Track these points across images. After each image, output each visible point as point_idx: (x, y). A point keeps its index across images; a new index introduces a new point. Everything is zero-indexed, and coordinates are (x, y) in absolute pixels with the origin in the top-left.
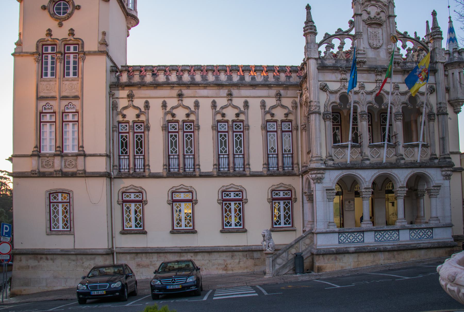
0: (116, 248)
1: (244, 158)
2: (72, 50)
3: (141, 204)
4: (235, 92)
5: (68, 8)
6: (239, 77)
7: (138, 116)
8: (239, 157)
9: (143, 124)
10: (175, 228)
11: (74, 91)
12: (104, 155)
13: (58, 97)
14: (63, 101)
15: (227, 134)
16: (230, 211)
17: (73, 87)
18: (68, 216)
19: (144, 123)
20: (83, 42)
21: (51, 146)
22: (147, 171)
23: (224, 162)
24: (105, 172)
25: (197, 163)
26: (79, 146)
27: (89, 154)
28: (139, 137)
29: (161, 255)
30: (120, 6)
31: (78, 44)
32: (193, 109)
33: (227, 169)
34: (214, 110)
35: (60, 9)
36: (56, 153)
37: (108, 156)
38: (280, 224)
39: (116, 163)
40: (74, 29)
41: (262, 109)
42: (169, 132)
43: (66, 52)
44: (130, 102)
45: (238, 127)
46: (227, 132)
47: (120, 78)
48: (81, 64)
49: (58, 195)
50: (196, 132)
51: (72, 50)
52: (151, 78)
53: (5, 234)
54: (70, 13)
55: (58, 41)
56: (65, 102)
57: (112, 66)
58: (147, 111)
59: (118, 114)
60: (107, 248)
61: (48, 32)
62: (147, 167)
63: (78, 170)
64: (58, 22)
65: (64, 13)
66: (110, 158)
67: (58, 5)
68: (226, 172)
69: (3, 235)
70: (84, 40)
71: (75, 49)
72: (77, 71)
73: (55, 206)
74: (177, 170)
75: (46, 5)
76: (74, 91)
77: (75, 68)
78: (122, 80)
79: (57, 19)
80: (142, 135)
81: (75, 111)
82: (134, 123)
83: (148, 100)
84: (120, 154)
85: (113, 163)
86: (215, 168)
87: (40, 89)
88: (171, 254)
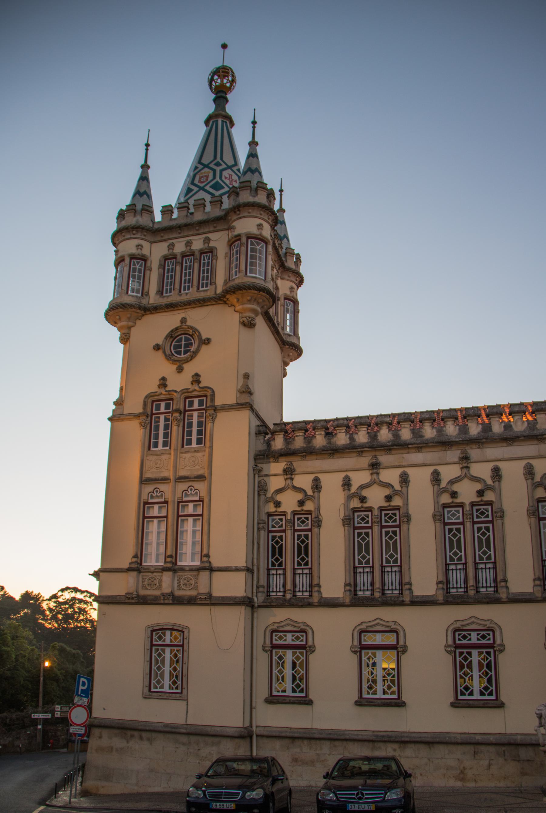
0: (257, 727)
1: (495, 568)
2: (196, 405)
3: (304, 651)
4: (474, 453)
5: (191, 344)
6: (480, 426)
8: (486, 568)
9: (309, 516)
10: (365, 696)
11: (197, 467)
12: (243, 568)
13: (172, 478)
14: (179, 484)
15: (461, 527)
16: (470, 666)
17: (196, 462)
18: (179, 669)
19: (311, 514)
20: (213, 392)
21: (158, 555)
22: (315, 594)
23: (456, 577)
24: (245, 597)
25: (406, 579)
26: (203, 554)
27: (218, 567)
28: (303, 537)
29: (338, 743)
30: (272, 332)
31: (206, 396)
32: (397, 487)
33: (462, 590)
34: (436, 487)
36: (165, 566)
37: (249, 570)
39: (263, 582)
40: (200, 373)
41: (526, 480)
42: (355, 528)
43: (187, 408)
44: (289, 481)
45: (482, 513)
46: (462, 523)
47: (272, 443)
49: (165, 632)
50: (404, 527)
51: (196, 405)
52: (324, 439)
53: (81, 693)
54: (194, 350)
55: (175, 394)
57: (258, 426)
58: (316, 494)
59: (267, 501)
60: (242, 726)
61: (162, 381)
62: (316, 589)
63: (199, 594)
64: (177, 366)
65: (186, 352)
66: (253, 574)
67: (178, 341)
68: (461, 595)
69: (77, 694)
70: (214, 389)
71: (201, 403)
72: (203, 436)
73: (160, 651)
74: (368, 593)
75: (160, 343)
76: (197, 467)
77: (199, 433)
78: (275, 446)
79: (174, 362)
80: (308, 535)
81: (197, 498)
82: (294, 515)
83: (319, 475)
84: (270, 567)
85: (258, 582)
86: (439, 589)
87: (146, 468)
88: (356, 744)
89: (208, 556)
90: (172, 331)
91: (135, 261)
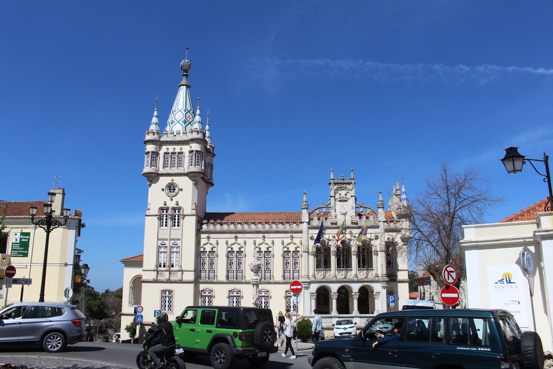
7: (212, 249)
35: (171, 189)
40: (178, 201)
56: (173, 241)
65: (173, 192)
75: (164, 188)
85: (197, 274)
89: (181, 266)
90: (168, 184)
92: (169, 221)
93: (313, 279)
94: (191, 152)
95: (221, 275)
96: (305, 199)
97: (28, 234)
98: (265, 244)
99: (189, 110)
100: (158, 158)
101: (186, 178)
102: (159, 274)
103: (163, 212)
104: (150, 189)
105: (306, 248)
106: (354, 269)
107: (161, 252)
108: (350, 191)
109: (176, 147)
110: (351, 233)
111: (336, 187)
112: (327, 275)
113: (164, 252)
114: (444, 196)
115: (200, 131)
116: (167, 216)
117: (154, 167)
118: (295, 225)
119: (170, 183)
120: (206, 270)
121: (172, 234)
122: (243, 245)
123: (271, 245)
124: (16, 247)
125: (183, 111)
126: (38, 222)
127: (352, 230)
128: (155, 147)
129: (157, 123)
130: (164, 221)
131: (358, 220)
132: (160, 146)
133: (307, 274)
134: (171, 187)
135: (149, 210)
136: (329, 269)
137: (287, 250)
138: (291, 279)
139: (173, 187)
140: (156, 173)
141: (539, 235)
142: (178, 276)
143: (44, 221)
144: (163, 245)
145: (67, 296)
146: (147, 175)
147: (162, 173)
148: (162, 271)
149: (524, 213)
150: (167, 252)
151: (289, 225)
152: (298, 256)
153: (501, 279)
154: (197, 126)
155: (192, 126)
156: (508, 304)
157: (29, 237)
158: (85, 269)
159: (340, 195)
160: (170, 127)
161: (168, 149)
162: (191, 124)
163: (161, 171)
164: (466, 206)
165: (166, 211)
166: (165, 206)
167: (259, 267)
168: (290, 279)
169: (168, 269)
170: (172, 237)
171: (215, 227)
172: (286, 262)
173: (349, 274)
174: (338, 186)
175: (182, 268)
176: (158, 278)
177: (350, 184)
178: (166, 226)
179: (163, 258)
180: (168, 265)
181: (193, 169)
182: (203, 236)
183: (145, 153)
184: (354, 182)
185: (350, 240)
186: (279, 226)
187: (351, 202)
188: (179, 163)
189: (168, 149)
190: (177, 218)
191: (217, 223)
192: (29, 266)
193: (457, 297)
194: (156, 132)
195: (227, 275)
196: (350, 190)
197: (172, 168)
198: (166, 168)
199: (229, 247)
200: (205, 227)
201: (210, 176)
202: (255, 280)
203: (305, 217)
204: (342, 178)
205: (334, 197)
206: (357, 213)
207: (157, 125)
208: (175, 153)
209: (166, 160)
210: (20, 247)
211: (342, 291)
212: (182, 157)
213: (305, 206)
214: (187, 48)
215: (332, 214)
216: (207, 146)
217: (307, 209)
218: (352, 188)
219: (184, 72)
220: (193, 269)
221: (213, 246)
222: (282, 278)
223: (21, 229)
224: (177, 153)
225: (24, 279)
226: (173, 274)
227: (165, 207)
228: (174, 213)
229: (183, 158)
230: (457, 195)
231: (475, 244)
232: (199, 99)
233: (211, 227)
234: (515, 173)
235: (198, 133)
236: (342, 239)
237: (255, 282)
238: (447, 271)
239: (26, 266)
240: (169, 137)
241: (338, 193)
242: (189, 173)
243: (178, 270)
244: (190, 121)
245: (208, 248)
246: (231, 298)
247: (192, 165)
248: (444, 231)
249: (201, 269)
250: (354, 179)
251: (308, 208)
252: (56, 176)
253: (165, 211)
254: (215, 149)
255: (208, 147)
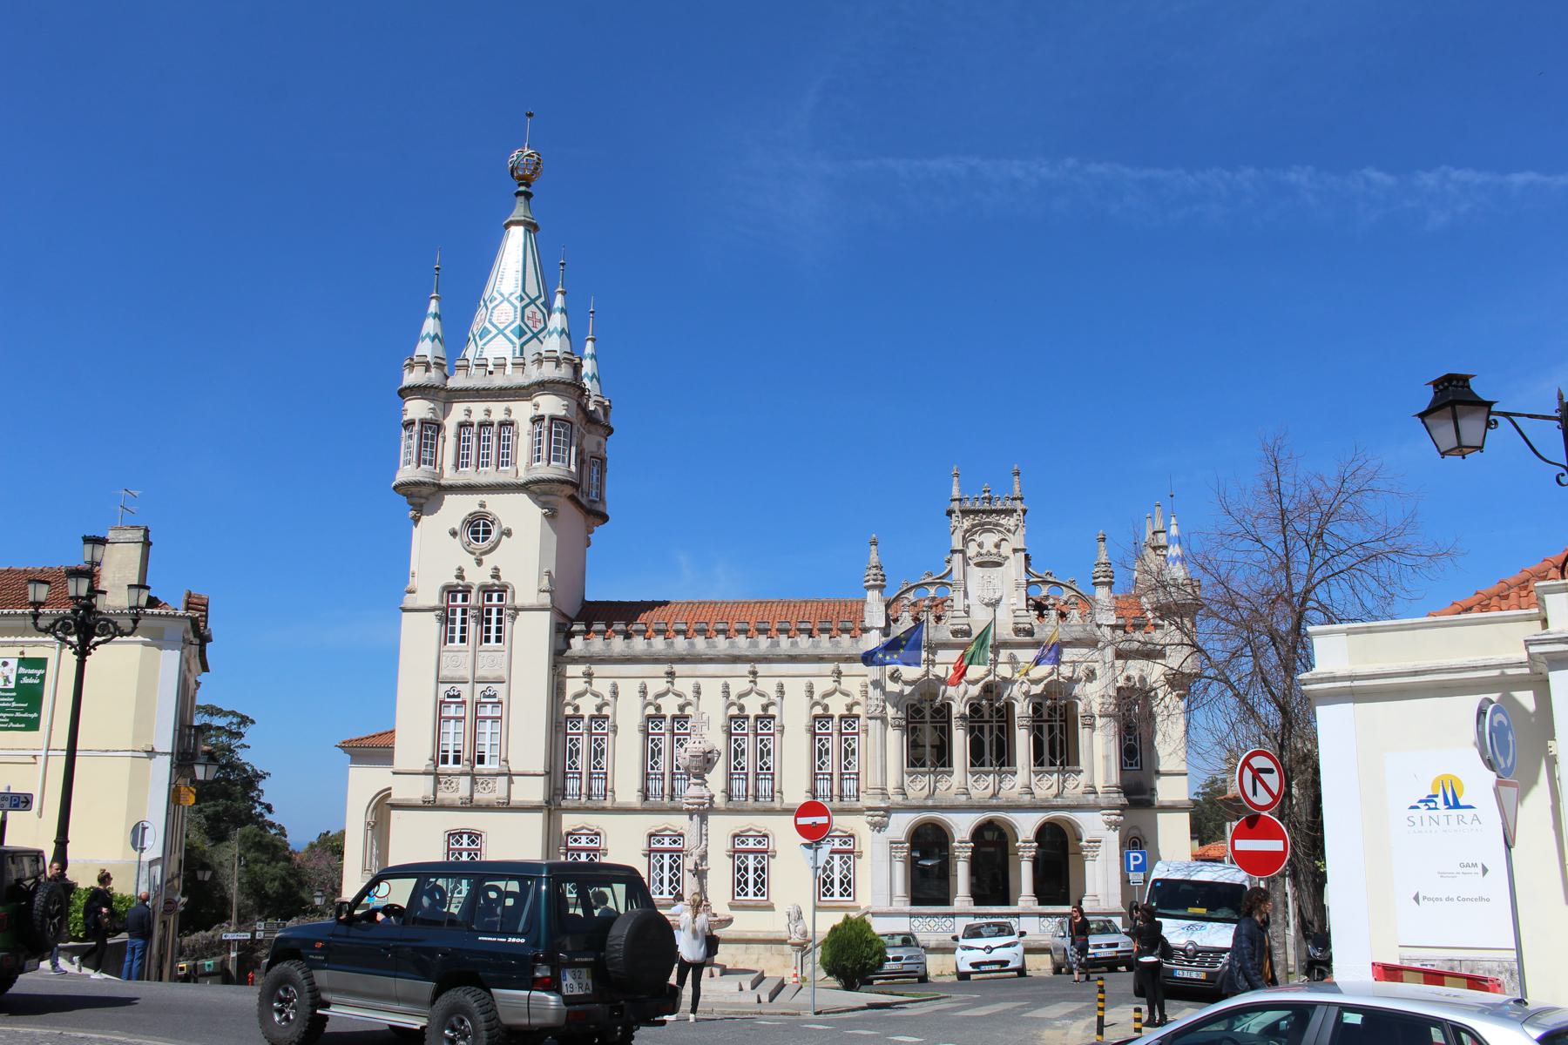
7: (599, 708)
38: (832, 895)
48: (508, 625)
56: (480, 687)
57: (559, 624)
65: (484, 540)
75: (457, 527)
89: (506, 761)
90: (470, 515)
91: (427, 425)
92: (472, 626)
93: (899, 799)
94: (537, 420)
95: (627, 788)
96: (874, 558)
97: (41, 663)
98: (757, 693)
99: (533, 297)
100: (440, 440)
101: (523, 499)
102: (439, 783)
103: (454, 599)
104: (416, 531)
105: (878, 706)
106: (1023, 768)
107: (449, 719)
108: (1011, 535)
109: (493, 406)
110: (1013, 661)
111: (967, 523)
112: (942, 786)
113: (458, 719)
114: (1275, 541)
115: (565, 359)
116: (464, 612)
117: (427, 466)
118: (846, 636)
119: (475, 513)
120: (581, 773)
121: (480, 666)
122: (690, 696)
123: (774, 696)
124: (6, 702)
125: (516, 298)
126: (53, 625)
127: (1015, 652)
128: (432, 405)
129: (436, 336)
130: (458, 626)
131: (1036, 623)
132: (445, 403)
133: (879, 784)
134: (479, 526)
135: (414, 592)
136: (947, 769)
137: (821, 712)
138: (836, 799)
139: (485, 525)
140: (434, 484)
141: (1541, 654)
142: (495, 791)
143: (70, 621)
144: (454, 696)
145: (139, 846)
146: (406, 489)
147: (450, 482)
148: (450, 775)
149: (1510, 587)
150: (464, 718)
151: (830, 638)
152: (856, 731)
153: (1429, 796)
154: (554, 343)
155: (542, 343)
156: (1452, 875)
157: (43, 672)
158: (206, 765)
159: (980, 545)
160: (477, 346)
161: (470, 411)
162: (538, 339)
163: (449, 476)
164: (1342, 572)
165: (463, 595)
166: (461, 582)
167: (709, 760)
168: (831, 801)
169: (468, 769)
170: (480, 673)
171: (608, 645)
172: (820, 750)
173: (1006, 785)
174: (974, 520)
175: (510, 765)
176: (440, 795)
177: (1009, 512)
178: (463, 640)
179: (452, 735)
180: (466, 755)
181: (544, 470)
182: (572, 670)
183: (403, 424)
184: (1023, 507)
185: (1007, 682)
186: (799, 639)
187: (1014, 568)
188: (503, 453)
189: (469, 412)
190: (494, 616)
191: (615, 631)
192: (43, 758)
193: (1282, 849)
194: (435, 363)
195: (643, 788)
196: (1009, 531)
197: (480, 468)
198: (464, 469)
199: (650, 704)
200: (577, 643)
201: (597, 493)
202: (694, 797)
203: (875, 614)
204: (987, 494)
205: (962, 552)
206: (1031, 602)
207: (437, 340)
208: (492, 424)
209: (464, 446)
210: (17, 700)
211: (988, 835)
212: (511, 435)
213: (874, 580)
214: (530, 115)
215: (955, 603)
216: (587, 404)
217: (881, 588)
218: (1017, 525)
219: (520, 185)
220: (541, 769)
221: (603, 700)
222: (807, 797)
223: (21, 649)
224: (495, 425)
225: (9, 796)
226: (482, 783)
227: (458, 585)
228: (486, 603)
229: (515, 438)
230: (1315, 540)
231: (1348, 684)
232: (563, 264)
233: (597, 645)
234: (1464, 458)
235: (558, 362)
236: (986, 679)
237: (696, 806)
238: (1251, 767)
239: (34, 757)
240: (471, 377)
241: (974, 540)
242: (530, 482)
243: (496, 771)
244: (535, 330)
245: (588, 707)
246: (655, 857)
247: (538, 461)
248: (1272, 651)
249: (567, 770)
250: (1021, 499)
251: (884, 586)
252: (124, 492)
253: (460, 596)
254: (612, 414)
255: (592, 408)
